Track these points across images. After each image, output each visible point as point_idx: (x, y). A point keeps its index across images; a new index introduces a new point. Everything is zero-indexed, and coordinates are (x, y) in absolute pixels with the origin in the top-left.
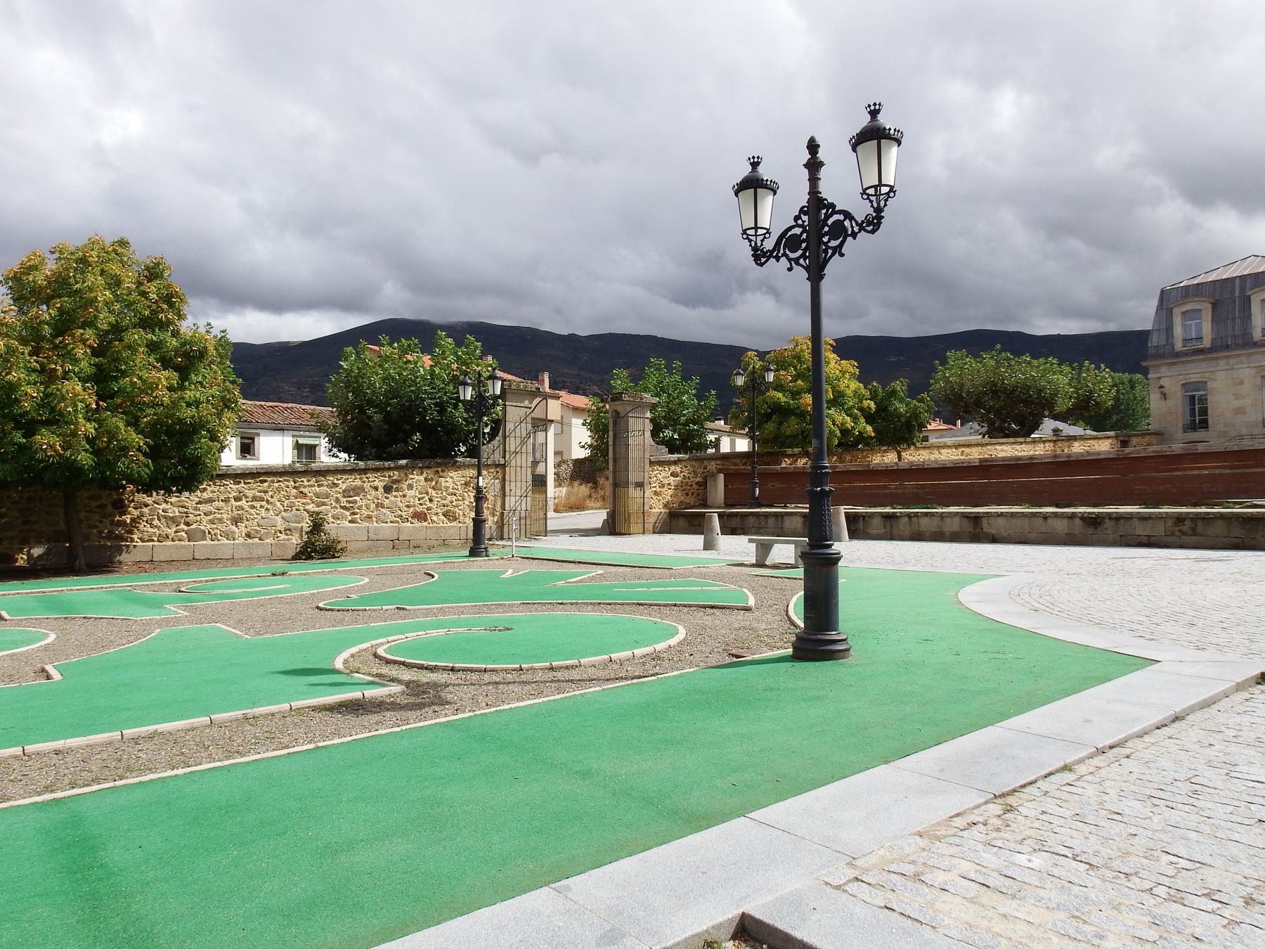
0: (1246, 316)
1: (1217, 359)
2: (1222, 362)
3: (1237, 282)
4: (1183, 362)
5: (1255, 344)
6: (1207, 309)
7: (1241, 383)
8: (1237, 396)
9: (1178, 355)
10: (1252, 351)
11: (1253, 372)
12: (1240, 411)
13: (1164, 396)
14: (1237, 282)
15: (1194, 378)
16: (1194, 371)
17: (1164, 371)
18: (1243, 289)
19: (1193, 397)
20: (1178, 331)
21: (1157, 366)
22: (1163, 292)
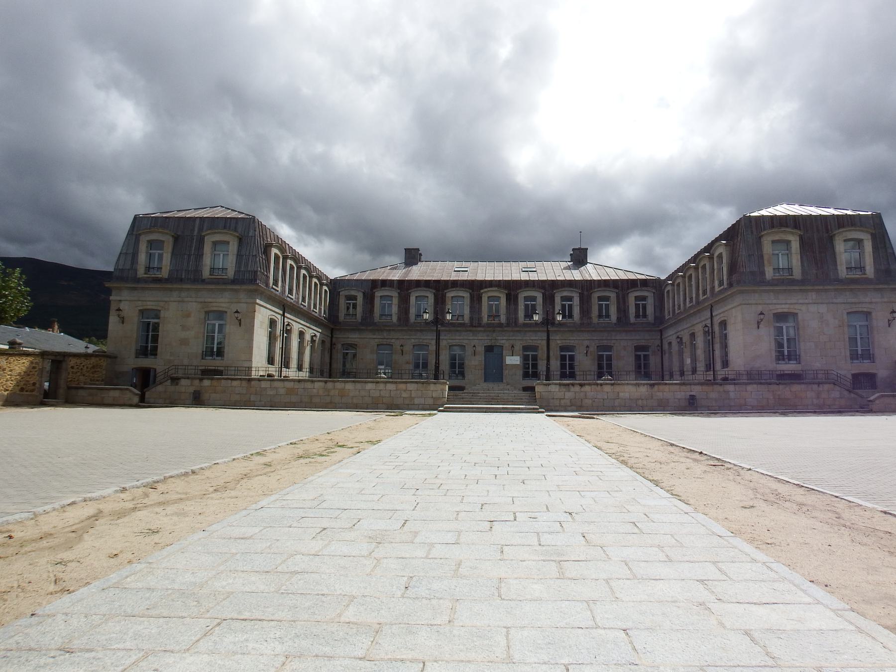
0: (200, 256)
1: (171, 290)
3: (198, 222)
4: (143, 289)
5: (203, 281)
7: (188, 316)
8: (184, 328)
10: (199, 287)
12: (184, 342)
13: (122, 320)
14: (198, 222)
15: (150, 305)
16: (150, 299)
17: (125, 295)
18: (201, 230)
19: (149, 324)
20: (142, 258)
21: (120, 289)
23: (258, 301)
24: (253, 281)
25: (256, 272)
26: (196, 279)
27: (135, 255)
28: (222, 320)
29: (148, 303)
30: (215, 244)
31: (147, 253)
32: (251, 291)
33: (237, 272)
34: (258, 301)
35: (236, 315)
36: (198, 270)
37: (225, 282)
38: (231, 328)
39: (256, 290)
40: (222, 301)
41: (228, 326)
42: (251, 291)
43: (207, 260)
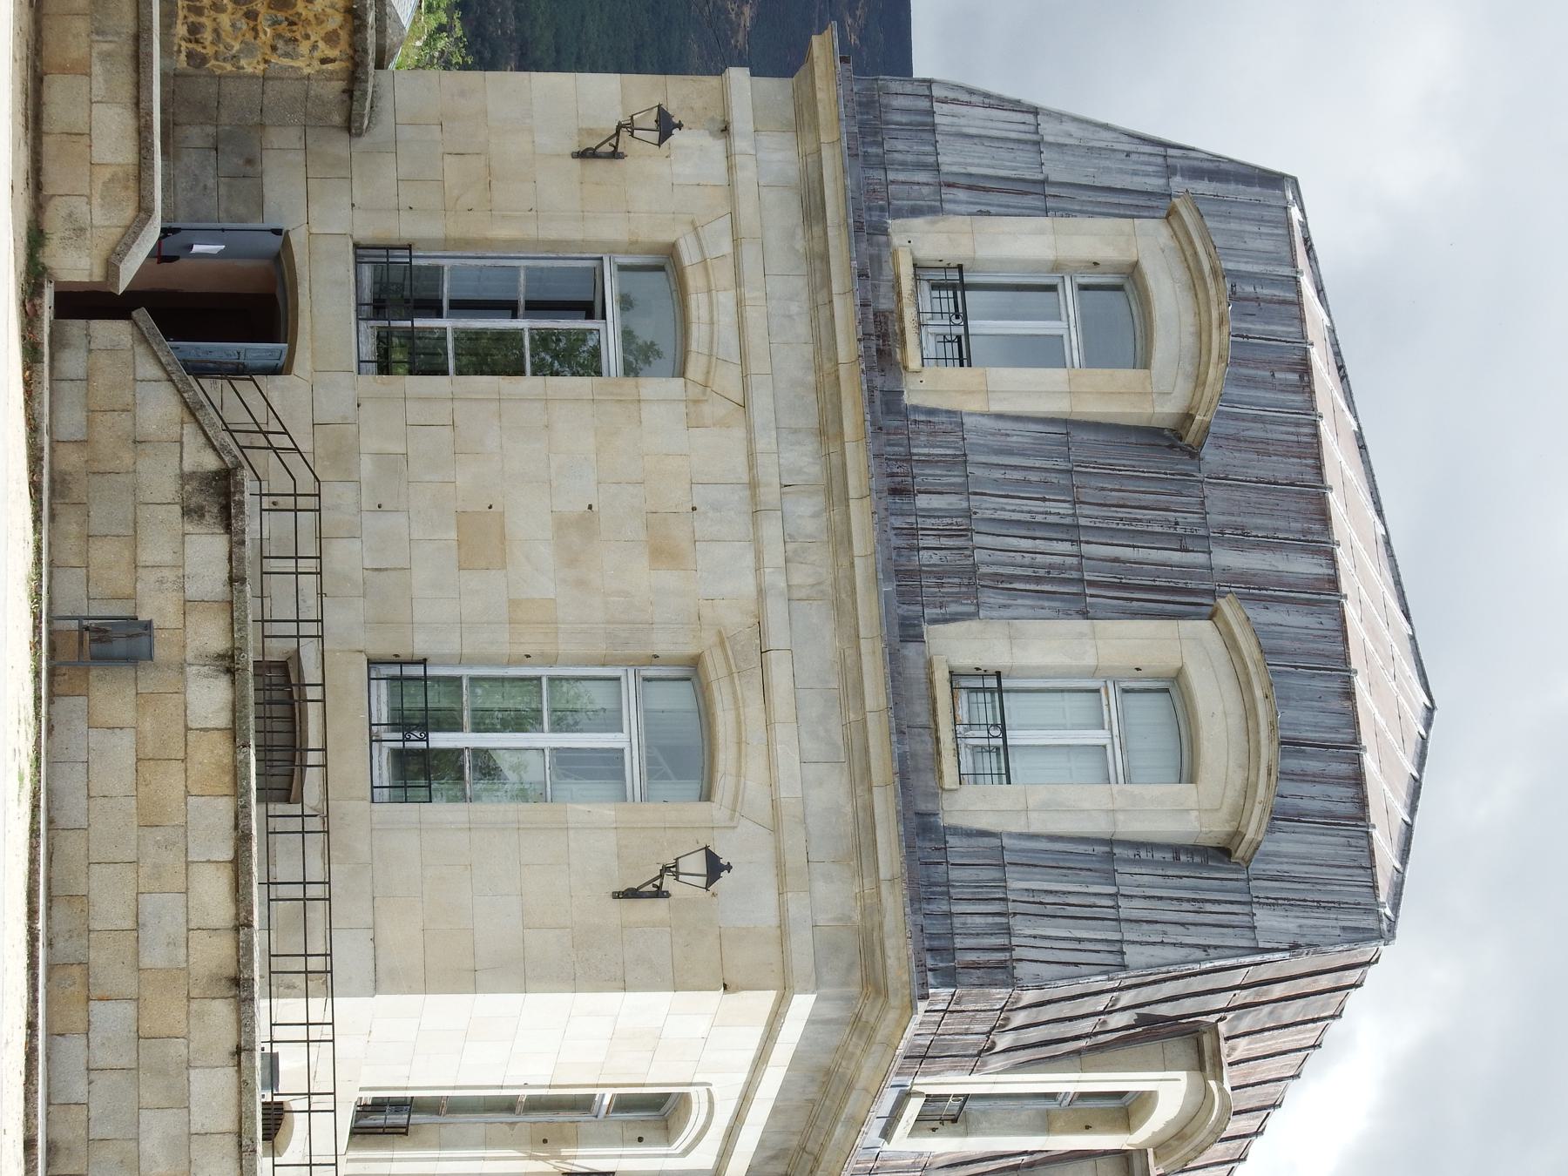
0: (1076, 595)
1: (828, 431)
2: (803, 458)
3: (1305, 566)
4: (819, 259)
5: (907, 632)
6: (1154, 393)
7: (662, 553)
9: (868, 228)
11: (735, 619)
12: (480, 538)
14: (1305, 566)
15: (711, 310)
16: (758, 310)
18: (1255, 590)
21: (803, 119)
22: (1274, 180)
23: (802, 1005)
24: (941, 961)
25: (1002, 972)
26: (919, 586)
27: (1034, 195)
28: (653, 771)
29: (726, 299)
30: (1171, 688)
31: (1057, 267)
32: (868, 949)
33: (995, 851)
34: (802, 1005)
35: (696, 864)
36: (972, 589)
37: (914, 775)
38: (598, 835)
39: (875, 986)
40: (787, 763)
41: (607, 812)
42: (868, 949)
43: (1043, 645)
